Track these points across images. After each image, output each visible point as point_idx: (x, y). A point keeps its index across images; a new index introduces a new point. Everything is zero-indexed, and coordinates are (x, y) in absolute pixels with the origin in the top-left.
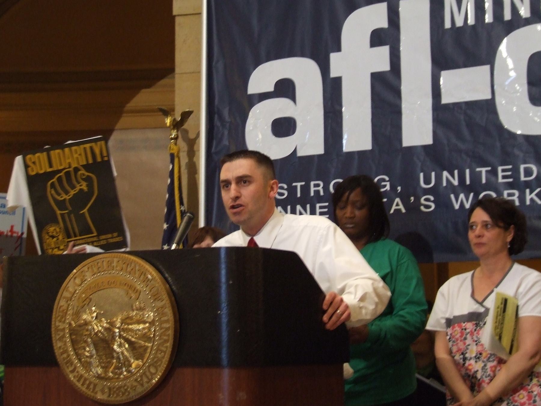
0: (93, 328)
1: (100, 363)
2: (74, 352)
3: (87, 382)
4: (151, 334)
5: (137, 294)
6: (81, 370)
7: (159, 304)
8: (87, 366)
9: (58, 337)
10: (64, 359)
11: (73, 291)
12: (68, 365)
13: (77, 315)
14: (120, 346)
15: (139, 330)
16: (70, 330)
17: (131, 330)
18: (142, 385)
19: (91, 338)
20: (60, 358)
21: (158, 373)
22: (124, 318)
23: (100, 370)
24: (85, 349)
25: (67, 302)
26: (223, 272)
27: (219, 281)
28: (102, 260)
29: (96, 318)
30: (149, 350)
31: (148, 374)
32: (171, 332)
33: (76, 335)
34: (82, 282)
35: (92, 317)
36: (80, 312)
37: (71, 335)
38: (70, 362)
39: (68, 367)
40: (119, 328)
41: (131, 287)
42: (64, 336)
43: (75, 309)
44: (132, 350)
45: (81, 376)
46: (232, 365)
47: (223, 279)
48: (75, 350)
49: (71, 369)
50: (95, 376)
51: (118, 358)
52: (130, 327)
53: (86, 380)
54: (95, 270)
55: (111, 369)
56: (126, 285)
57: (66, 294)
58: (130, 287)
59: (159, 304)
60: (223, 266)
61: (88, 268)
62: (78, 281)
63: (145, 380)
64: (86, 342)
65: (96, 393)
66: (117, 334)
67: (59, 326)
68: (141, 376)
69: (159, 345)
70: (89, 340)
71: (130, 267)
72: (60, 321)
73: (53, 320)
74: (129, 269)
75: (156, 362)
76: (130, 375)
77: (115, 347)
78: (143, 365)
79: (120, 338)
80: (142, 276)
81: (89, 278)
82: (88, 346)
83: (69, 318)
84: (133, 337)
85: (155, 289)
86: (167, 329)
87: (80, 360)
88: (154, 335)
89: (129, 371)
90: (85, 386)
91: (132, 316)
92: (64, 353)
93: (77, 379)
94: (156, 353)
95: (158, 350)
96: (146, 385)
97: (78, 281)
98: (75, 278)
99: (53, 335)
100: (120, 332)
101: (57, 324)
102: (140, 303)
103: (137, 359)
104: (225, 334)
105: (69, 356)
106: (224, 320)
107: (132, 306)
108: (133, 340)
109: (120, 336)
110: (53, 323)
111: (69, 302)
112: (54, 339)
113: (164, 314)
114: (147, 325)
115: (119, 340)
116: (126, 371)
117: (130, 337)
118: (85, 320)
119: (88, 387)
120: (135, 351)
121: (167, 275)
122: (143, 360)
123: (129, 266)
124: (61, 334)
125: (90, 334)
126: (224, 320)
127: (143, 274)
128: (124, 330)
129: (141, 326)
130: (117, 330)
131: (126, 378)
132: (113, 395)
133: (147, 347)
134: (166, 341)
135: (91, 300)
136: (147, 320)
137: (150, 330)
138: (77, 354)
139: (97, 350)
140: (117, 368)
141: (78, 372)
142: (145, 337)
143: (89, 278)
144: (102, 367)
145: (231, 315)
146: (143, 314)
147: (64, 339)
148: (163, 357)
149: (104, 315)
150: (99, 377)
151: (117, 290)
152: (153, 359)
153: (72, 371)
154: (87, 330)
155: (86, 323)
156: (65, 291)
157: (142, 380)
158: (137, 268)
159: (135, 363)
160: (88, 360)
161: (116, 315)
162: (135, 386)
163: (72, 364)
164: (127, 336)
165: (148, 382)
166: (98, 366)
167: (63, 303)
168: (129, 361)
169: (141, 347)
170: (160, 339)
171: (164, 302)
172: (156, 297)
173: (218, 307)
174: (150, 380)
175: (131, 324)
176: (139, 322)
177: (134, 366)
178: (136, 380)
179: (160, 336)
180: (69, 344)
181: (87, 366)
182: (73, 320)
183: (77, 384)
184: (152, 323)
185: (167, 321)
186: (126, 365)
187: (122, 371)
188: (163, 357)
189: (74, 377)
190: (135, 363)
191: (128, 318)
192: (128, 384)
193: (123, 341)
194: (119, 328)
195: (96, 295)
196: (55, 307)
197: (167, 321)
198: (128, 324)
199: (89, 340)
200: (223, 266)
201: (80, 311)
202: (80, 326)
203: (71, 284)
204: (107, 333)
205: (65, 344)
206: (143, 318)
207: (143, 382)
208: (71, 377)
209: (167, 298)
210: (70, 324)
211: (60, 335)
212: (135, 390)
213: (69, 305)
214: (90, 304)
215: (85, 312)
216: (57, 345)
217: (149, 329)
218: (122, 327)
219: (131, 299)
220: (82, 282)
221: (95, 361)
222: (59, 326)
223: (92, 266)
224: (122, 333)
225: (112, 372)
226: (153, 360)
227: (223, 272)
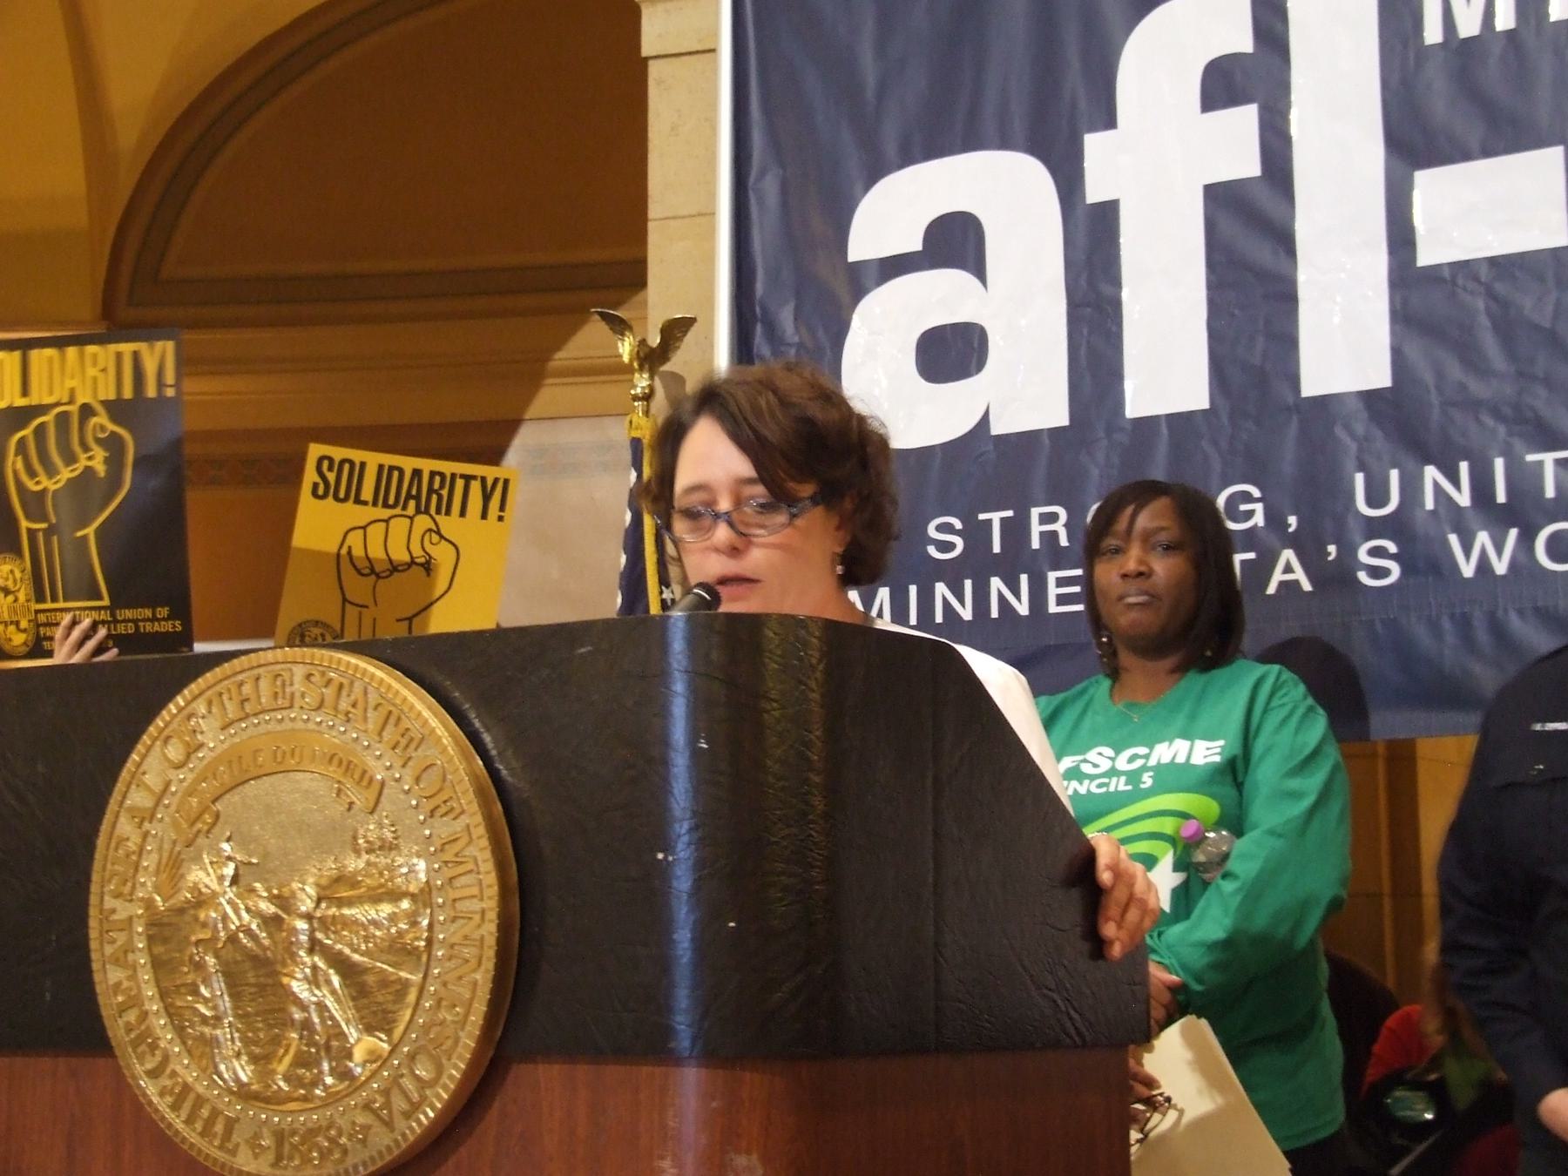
0: (225, 918)
1: (246, 1041)
2: (161, 1005)
3: (205, 1112)
4: (417, 939)
5: (372, 795)
6: (186, 1070)
7: (444, 828)
9: (109, 950)
10: (129, 1028)
11: (158, 788)
12: (140, 1049)
13: (174, 868)
14: (314, 980)
15: (375, 923)
16: (150, 925)
18: (389, 1124)
19: (217, 957)
20: (118, 1029)
21: (441, 1082)
22: (324, 882)
24: (195, 992)
25: (140, 826)
26: (679, 709)
27: (665, 742)
28: (256, 672)
29: (235, 880)
30: (412, 997)
31: (407, 1083)
33: (165, 941)
34: (192, 749)
35: (221, 878)
36: (183, 860)
37: (151, 939)
38: (148, 1042)
39: (142, 1062)
40: (308, 917)
41: (348, 767)
42: (129, 948)
43: (167, 846)
44: (354, 999)
45: (186, 1088)
46: (712, 1054)
47: (679, 731)
48: (163, 995)
50: (230, 1091)
51: (307, 1025)
52: (346, 911)
53: (200, 1101)
54: (232, 710)
55: (282, 1068)
56: (335, 761)
57: (137, 798)
58: (348, 768)
60: (679, 686)
61: (210, 703)
62: (174, 752)
63: (399, 1103)
64: (199, 966)
65: (233, 1152)
66: (304, 938)
67: (113, 911)
68: (386, 1093)
70: (211, 960)
71: (349, 696)
72: (118, 895)
73: (94, 888)
74: (344, 705)
76: (349, 1086)
77: (299, 988)
78: (392, 1052)
79: (311, 951)
80: (390, 728)
81: (213, 739)
82: (206, 981)
83: (146, 881)
84: (355, 951)
85: (434, 774)
87: (180, 1031)
88: (429, 941)
89: (344, 1075)
90: (199, 1126)
91: (356, 873)
92: (131, 1007)
93: (169, 1099)
96: (400, 1123)
97: (174, 752)
98: (168, 738)
99: (94, 945)
100: (312, 931)
101: (109, 902)
102: (381, 826)
103: (369, 1029)
104: (683, 938)
105: (145, 1015)
106: (682, 881)
107: (355, 838)
108: (356, 957)
109: (314, 946)
110: (93, 900)
111: (147, 825)
112: (94, 956)
114: (405, 904)
115: (307, 960)
116: (332, 1072)
117: (347, 951)
118: (195, 888)
119: (206, 1132)
120: (365, 1001)
121: (477, 724)
122: (389, 1032)
123: (344, 693)
124: (121, 938)
125: (215, 939)
126: (682, 881)
127: (392, 720)
128: (325, 924)
129: (386, 909)
130: (301, 925)
131: (333, 1098)
132: (291, 1158)
133: (406, 984)
135: (217, 816)
136: (404, 888)
138: (171, 1012)
139: (235, 996)
140: (302, 1061)
141: (174, 1074)
142: (399, 950)
143: (213, 739)
144: (254, 1059)
146: (391, 868)
147: (130, 957)
148: (463, 1022)
149: (260, 871)
150: (243, 1093)
152: (426, 1028)
153: (154, 1074)
154: (204, 925)
155: (202, 900)
156: (133, 787)
157: (387, 1104)
158: (373, 698)
159: (363, 1045)
160: (207, 1030)
161: (296, 870)
162: (366, 1128)
163: (154, 1047)
164: (339, 946)
165: (407, 1115)
166: (238, 1055)
167: (125, 827)
168: (342, 1036)
171: (464, 820)
174: (416, 1107)
175: (350, 902)
176: (376, 897)
177: (359, 1054)
178: (367, 1107)
182: (157, 889)
183: (170, 1116)
184: (423, 897)
186: (334, 1051)
187: (321, 1072)
189: (162, 1094)
190: (363, 1045)
191: (339, 880)
192: (340, 1121)
193: (321, 964)
194: (308, 917)
195: (234, 798)
196: (101, 842)
198: (341, 903)
199: (211, 960)
200: (679, 686)
201: (183, 856)
202: (181, 911)
203: (153, 762)
204: (270, 935)
205: (133, 977)
206: (391, 879)
207: (390, 1112)
208: (150, 1088)
209: (475, 807)
210: (149, 904)
211: (119, 943)
212: (364, 1142)
213: (146, 835)
214: (216, 830)
215: (197, 859)
216: (108, 977)
218: (318, 914)
219: (352, 812)
220: (188, 756)
221: (226, 1034)
222: (113, 911)
223: (221, 694)
224: (319, 935)
225: (286, 1079)
226: (427, 1033)
227: (679, 709)
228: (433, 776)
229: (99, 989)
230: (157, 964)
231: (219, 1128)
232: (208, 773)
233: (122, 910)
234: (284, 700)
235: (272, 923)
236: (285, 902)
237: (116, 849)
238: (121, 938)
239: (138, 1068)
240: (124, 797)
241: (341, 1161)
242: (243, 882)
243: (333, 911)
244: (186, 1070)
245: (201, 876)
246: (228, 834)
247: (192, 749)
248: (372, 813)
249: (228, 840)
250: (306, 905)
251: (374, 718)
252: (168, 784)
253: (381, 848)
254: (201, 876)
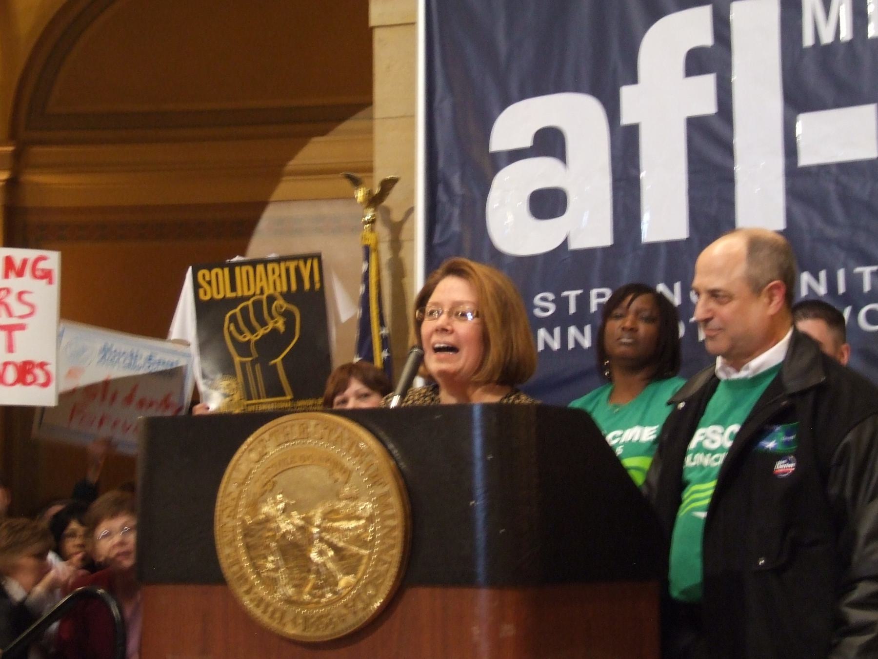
6: (261, 591)
7: (380, 490)
8: (272, 583)
10: (234, 573)
13: (254, 506)
14: (321, 553)
15: (348, 529)
17: (337, 530)
18: (355, 613)
20: (229, 571)
23: (290, 591)
27: (471, 455)
30: (365, 561)
32: (398, 534)
34: (262, 455)
38: (244, 579)
41: (336, 465)
46: (493, 582)
48: (251, 559)
49: (245, 588)
51: (318, 573)
53: (268, 605)
55: (308, 589)
59: (380, 490)
62: (253, 456)
63: (360, 605)
64: (268, 547)
65: (284, 625)
69: (381, 552)
75: (376, 578)
83: (241, 512)
86: (393, 528)
87: (259, 575)
94: (376, 565)
95: (378, 560)
97: (253, 456)
105: (242, 568)
109: (321, 540)
113: (387, 506)
124: (230, 535)
129: (353, 524)
131: (330, 603)
134: (392, 547)
135: (274, 484)
144: (295, 586)
145: (490, 508)
148: (387, 571)
150: (289, 601)
151: (314, 469)
152: (373, 572)
153: (248, 592)
158: (346, 435)
161: (313, 506)
165: (364, 609)
169: (353, 555)
170: (382, 543)
172: (375, 480)
173: (471, 496)
174: (368, 605)
176: (349, 518)
178: (345, 606)
179: (383, 538)
180: (242, 551)
181: (272, 583)
184: (370, 519)
185: (392, 517)
188: (387, 571)
194: (318, 526)
197: (392, 517)
210: (244, 522)
216: (225, 553)
217: (365, 527)
221: (282, 576)
225: (310, 593)
230: (248, 547)
231: (277, 615)
234: (304, 434)
235: (301, 529)
236: (308, 521)
239: (240, 590)
241: (334, 628)
243: (329, 524)
244: (261, 591)
245: (267, 509)
246: (281, 491)
247: (262, 455)
248: (346, 483)
250: (318, 521)
251: (346, 445)
254: (267, 509)
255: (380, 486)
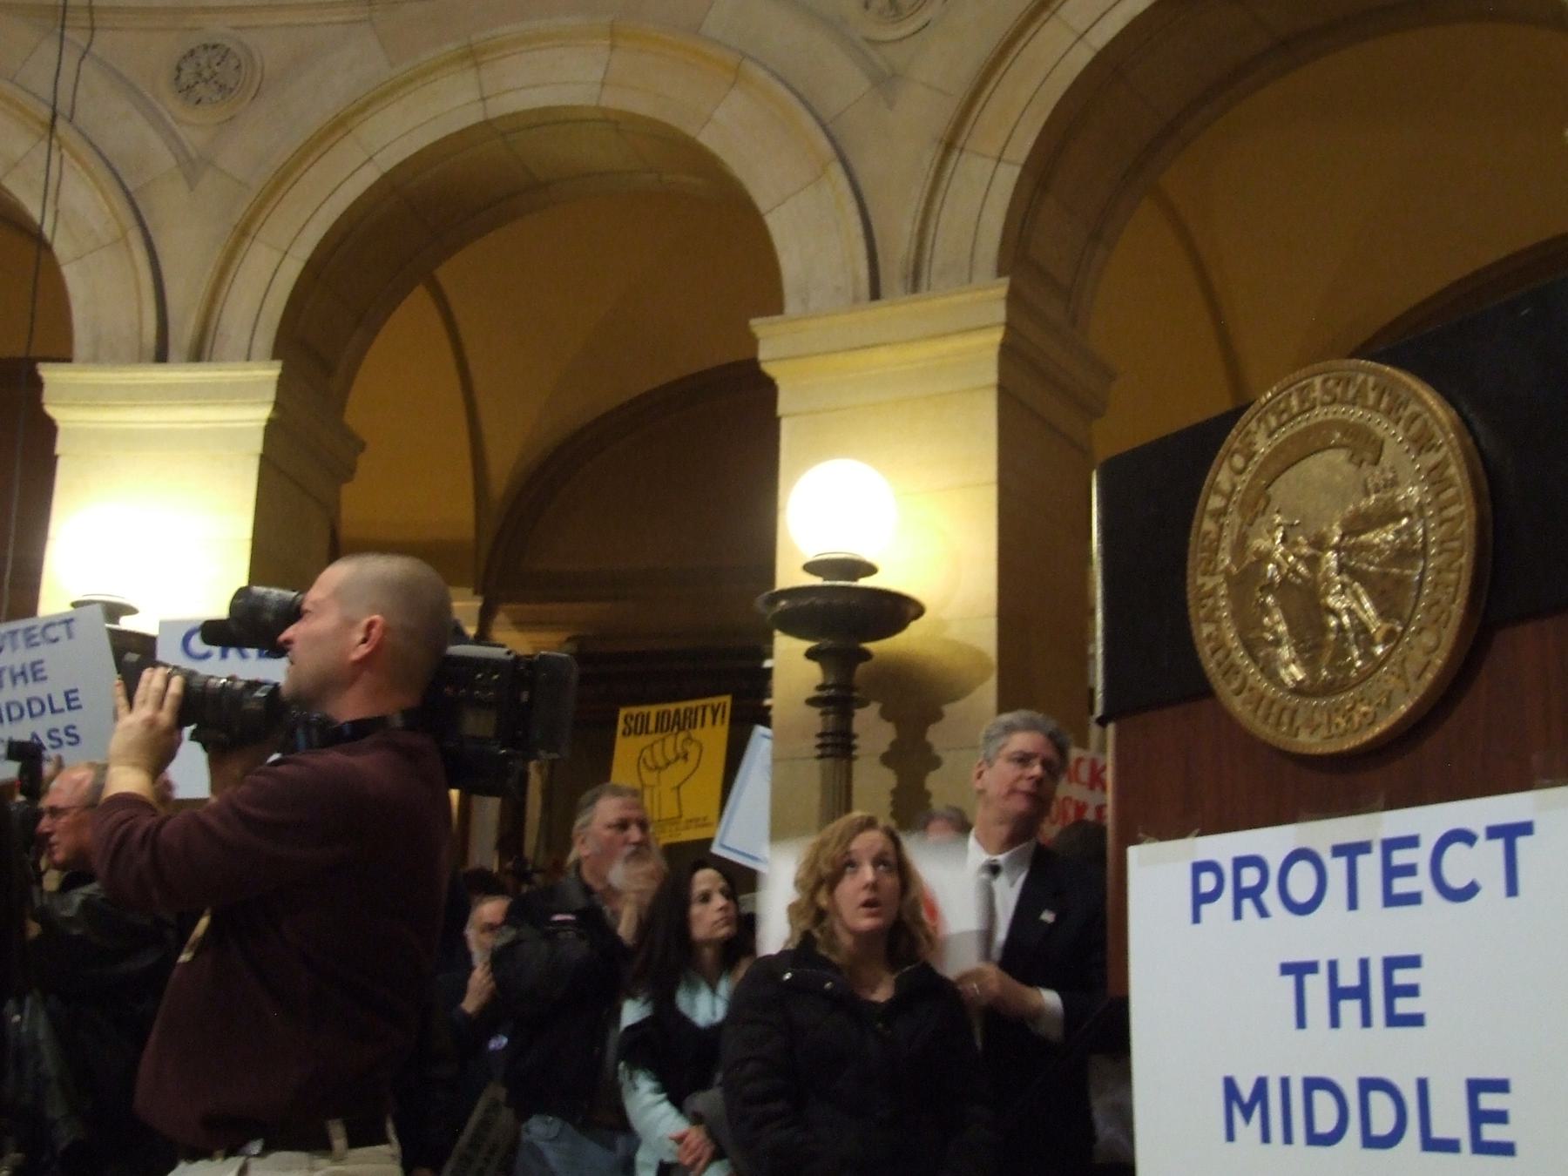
3: (1275, 709)
7: (1433, 458)
9: (1202, 613)
13: (1241, 545)
17: (1368, 547)
34: (1249, 457)
38: (1231, 670)
39: (1229, 683)
40: (1337, 548)
42: (1215, 608)
43: (1236, 530)
49: (1235, 685)
52: (1363, 537)
57: (1215, 502)
59: (1433, 458)
62: (1238, 461)
72: (1204, 574)
81: (1262, 447)
83: (1225, 559)
84: (1371, 563)
85: (1418, 425)
97: (1238, 461)
101: (1200, 581)
111: (1221, 520)
117: (1365, 566)
118: (1257, 552)
131: (1364, 676)
137: (1412, 534)
143: (1262, 447)
147: (1218, 613)
153: (1238, 692)
167: (1208, 525)
196: (1192, 539)
213: (1221, 528)
214: (1269, 509)
228: (1418, 425)
229: (1197, 640)
231: (1285, 718)
232: (1263, 466)
233: (1210, 583)
236: (1320, 543)
237: (1203, 541)
238: (1210, 602)
239: (1225, 689)
240: (1206, 503)
242: (1291, 539)
249: (1278, 512)
252: (1234, 486)
253: (1385, 486)
254: (1261, 543)
255: (1432, 453)
